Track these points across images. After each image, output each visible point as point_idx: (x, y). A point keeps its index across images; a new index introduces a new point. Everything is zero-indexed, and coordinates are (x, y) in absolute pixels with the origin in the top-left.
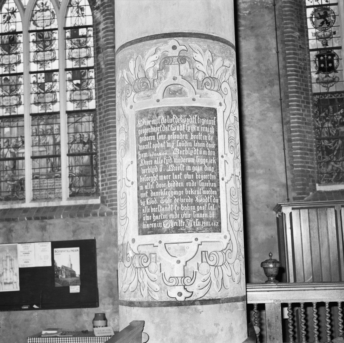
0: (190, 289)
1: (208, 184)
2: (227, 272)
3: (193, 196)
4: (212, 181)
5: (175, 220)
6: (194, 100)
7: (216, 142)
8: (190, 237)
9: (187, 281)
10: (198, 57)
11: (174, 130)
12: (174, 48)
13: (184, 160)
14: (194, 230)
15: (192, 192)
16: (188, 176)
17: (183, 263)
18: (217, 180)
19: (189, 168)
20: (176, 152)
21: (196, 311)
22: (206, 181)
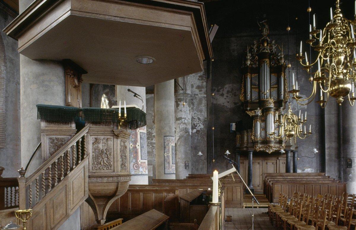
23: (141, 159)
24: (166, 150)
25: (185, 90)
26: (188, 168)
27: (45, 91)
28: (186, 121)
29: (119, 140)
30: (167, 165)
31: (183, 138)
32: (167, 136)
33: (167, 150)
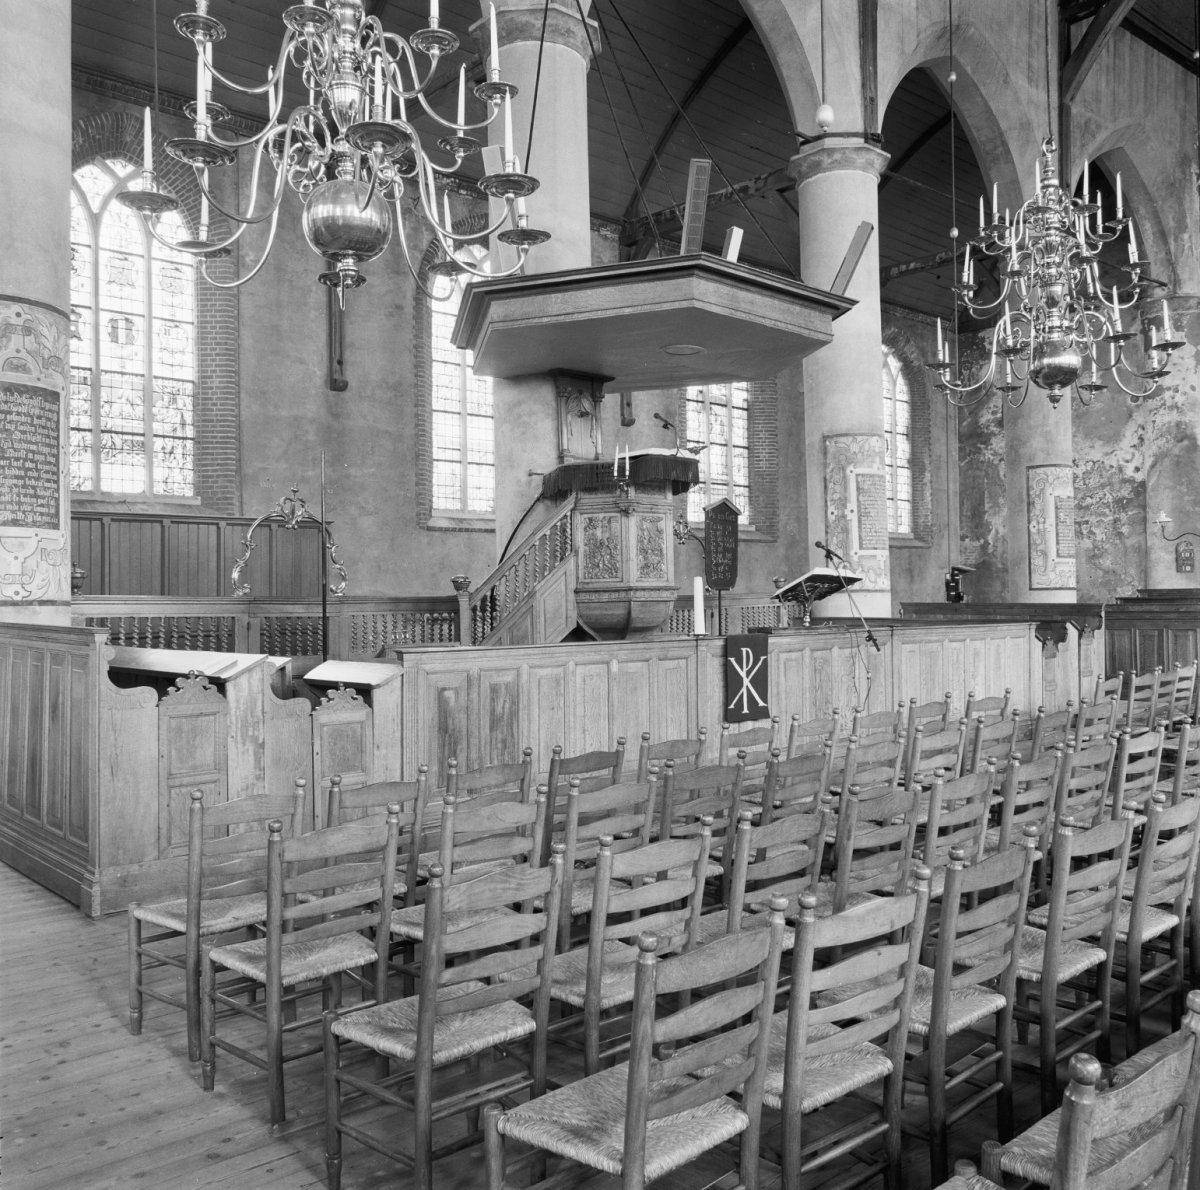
0: (28, 588)
1: (49, 476)
2: (63, 573)
3: (34, 488)
4: (54, 473)
5: (13, 512)
6: (39, 379)
7: (58, 430)
8: (31, 531)
9: (25, 579)
10: (45, 331)
11: (15, 409)
12: (18, 315)
13: (25, 446)
14: (34, 524)
15: (33, 482)
16: (29, 465)
17: (21, 559)
18: (56, 474)
19: (30, 456)
20: (17, 435)
21: (35, 612)
22: (47, 472)
23: (861, 548)
24: (1036, 511)
25: (1175, 286)
26: (1188, 568)
27: (524, 433)
28: (1179, 399)
29: (633, 522)
30: (1037, 561)
31: (1167, 462)
32: (1038, 467)
33: (1037, 513)
